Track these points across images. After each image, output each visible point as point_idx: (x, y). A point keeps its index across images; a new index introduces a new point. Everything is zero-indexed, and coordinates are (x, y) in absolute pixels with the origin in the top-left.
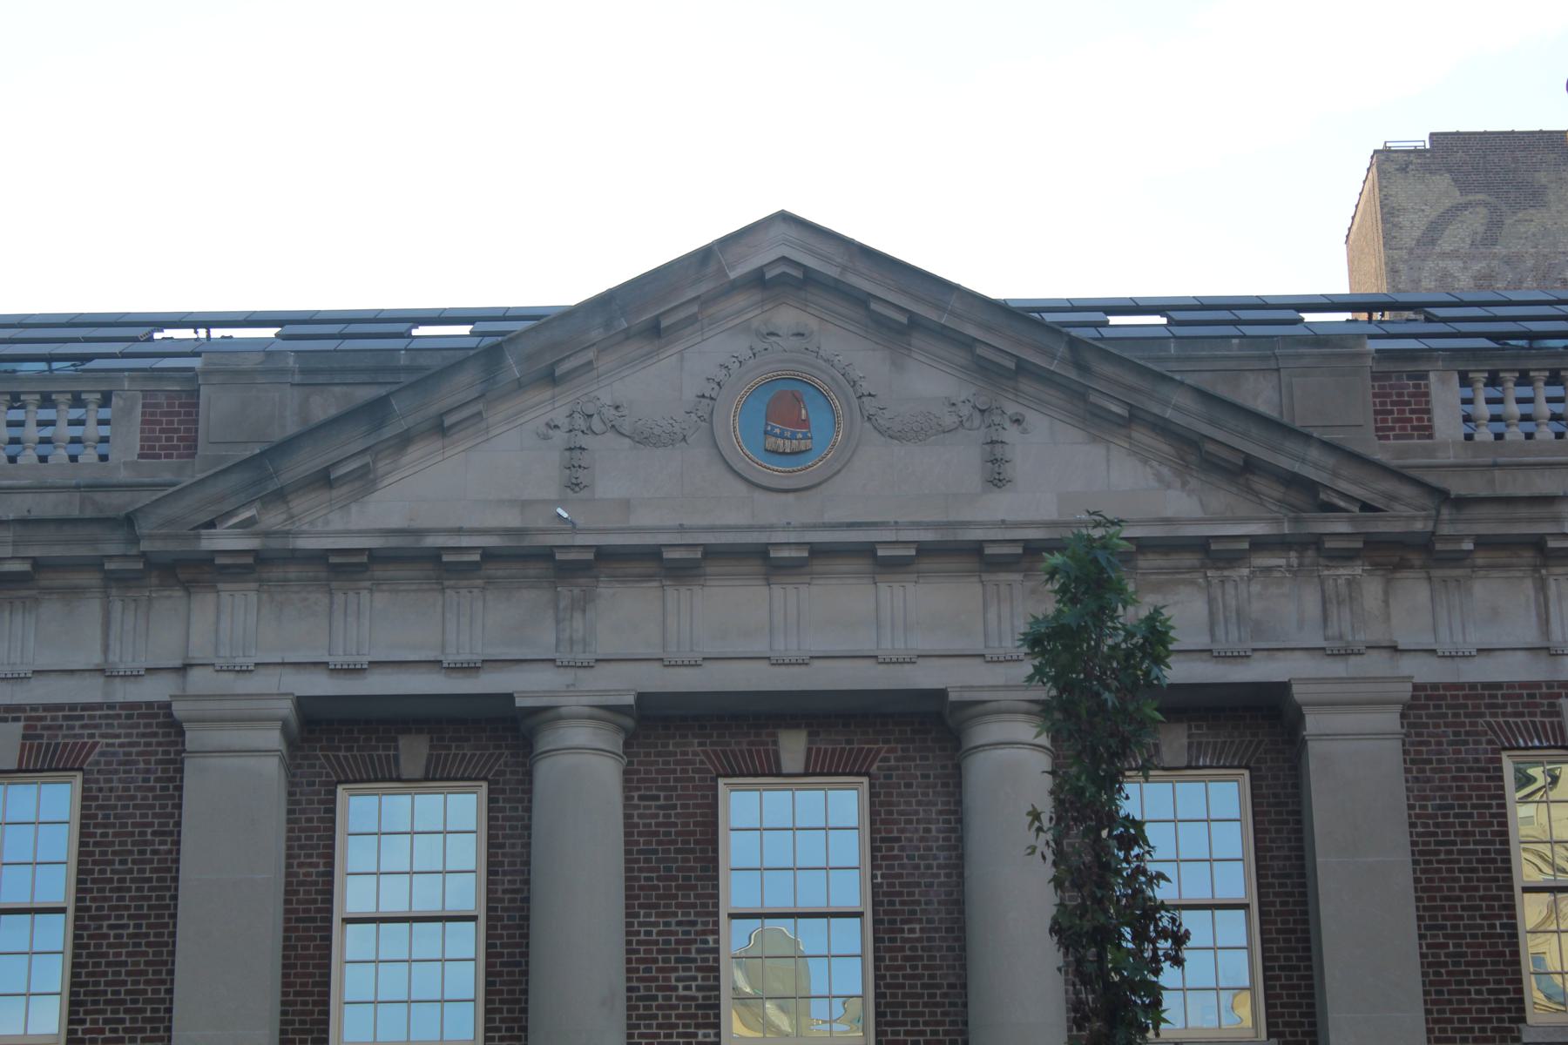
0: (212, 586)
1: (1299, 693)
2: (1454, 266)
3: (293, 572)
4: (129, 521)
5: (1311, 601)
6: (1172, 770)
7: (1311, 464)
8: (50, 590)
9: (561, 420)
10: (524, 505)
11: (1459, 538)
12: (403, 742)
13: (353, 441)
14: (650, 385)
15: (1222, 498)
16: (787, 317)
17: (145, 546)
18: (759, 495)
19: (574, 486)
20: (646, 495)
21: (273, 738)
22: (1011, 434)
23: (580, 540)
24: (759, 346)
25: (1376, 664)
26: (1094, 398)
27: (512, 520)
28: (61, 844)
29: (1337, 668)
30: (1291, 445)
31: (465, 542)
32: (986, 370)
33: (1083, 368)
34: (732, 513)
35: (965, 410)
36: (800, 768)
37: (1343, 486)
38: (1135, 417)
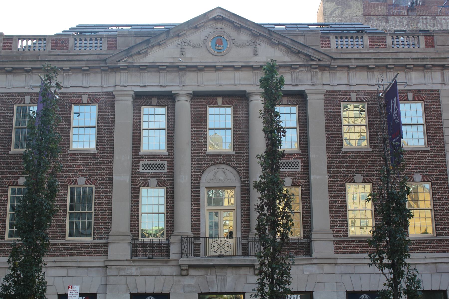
0: (120, 72)
1: (307, 92)
2: (335, 19)
3: (134, 69)
4: (105, 60)
5: (309, 76)
6: (284, 105)
7: (310, 52)
8: (92, 72)
9: (180, 43)
10: (174, 58)
11: (335, 65)
12: (153, 99)
13: (144, 47)
14: (195, 37)
15: (294, 58)
16: (219, 25)
17: (108, 65)
18: (214, 57)
19: (182, 55)
20: (195, 56)
21: (131, 98)
22: (258, 46)
23: (183, 64)
24: (214, 31)
25: (320, 87)
26: (272, 40)
27: (171, 60)
28: (95, 116)
29: (313, 88)
30: (306, 49)
31: (163, 64)
32: (254, 35)
33: (270, 35)
34: (210, 60)
35: (250, 42)
36: (221, 104)
37: (315, 56)
38: (279, 44)
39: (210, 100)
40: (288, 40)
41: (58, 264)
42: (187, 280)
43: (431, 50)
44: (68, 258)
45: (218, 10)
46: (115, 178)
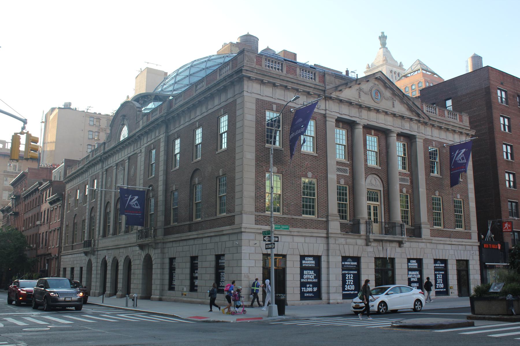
13: (344, 87)
14: (365, 87)
20: (366, 100)
25: (424, 135)
39: (368, 131)
40: (411, 102)
41: (300, 234)
42: (370, 249)
43: (462, 123)
44: (305, 230)
45: (380, 73)
46: (329, 176)
